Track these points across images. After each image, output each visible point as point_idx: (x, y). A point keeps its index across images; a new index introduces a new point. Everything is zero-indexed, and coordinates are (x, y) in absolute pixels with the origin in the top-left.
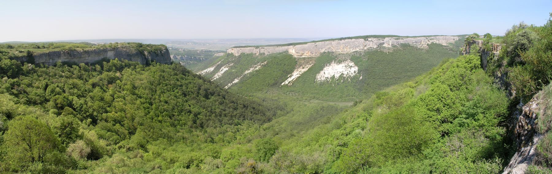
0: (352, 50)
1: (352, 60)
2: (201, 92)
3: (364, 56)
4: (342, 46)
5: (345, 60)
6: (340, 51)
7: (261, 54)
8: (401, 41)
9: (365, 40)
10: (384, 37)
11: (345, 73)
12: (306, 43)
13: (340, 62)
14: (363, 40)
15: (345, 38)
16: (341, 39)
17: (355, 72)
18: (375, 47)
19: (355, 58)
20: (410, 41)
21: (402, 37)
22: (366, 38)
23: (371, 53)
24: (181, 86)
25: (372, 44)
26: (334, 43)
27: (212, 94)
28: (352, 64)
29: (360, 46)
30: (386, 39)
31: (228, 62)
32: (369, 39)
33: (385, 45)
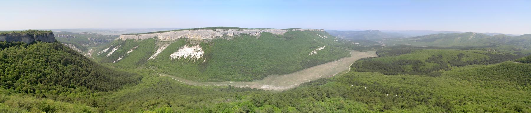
0: (203, 38)
1: (201, 46)
2: (62, 61)
3: (211, 43)
4: (195, 35)
5: (195, 45)
6: (193, 38)
7: (139, 40)
8: (241, 32)
9: (214, 31)
10: (228, 28)
11: (193, 55)
12: (169, 31)
13: (190, 46)
14: (211, 30)
15: (199, 29)
16: (195, 29)
17: (201, 55)
18: (221, 36)
19: (204, 45)
20: (247, 32)
21: (242, 29)
22: (214, 29)
23: (217, 40)
24: (48, 56)
25: (219, 34)
26: (190, 32)
27: (71, 63)
28: (200, 49)
29: (209, 36)
30: (230, 30)
31: (118, 45)
32: (217, 30)
33: (229, 35)
